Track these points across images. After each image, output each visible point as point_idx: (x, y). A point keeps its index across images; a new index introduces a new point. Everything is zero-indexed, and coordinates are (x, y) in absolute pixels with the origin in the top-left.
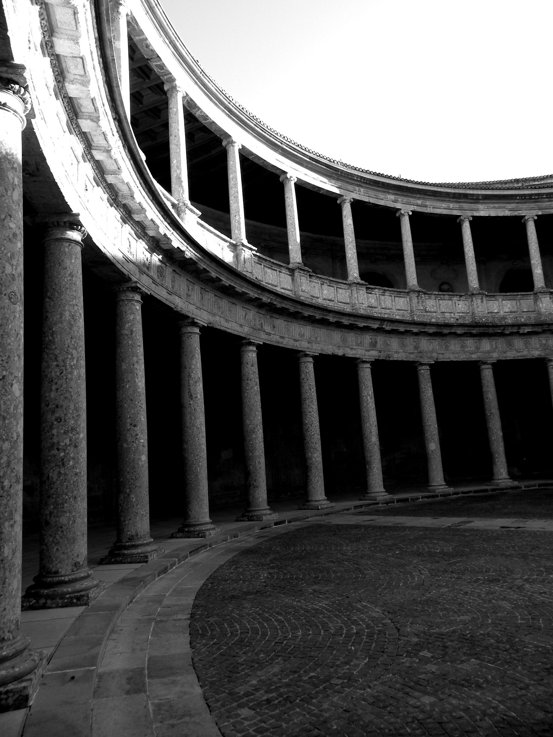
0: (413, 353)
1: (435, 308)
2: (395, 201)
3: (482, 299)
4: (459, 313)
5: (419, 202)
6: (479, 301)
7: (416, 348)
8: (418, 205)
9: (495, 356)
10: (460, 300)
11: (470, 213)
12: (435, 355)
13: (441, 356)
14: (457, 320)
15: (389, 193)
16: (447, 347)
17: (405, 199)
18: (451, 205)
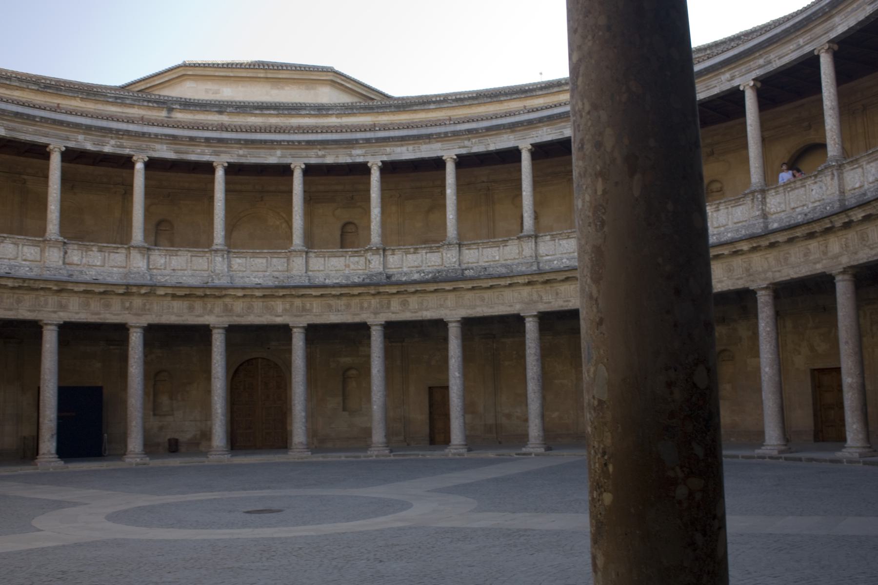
0: (741, 278)
1: (783, 206)
2: (732, 78)
3: (833, 174)
4: (813, 203)
5: (761, 61)
6: (829, 178)
7: (748, 270)
8: (760, 67)
9: (845, 261)
10: (816, 183)
11: (825, 39)
12: (770, 275)
13: (777, 275)
14: (806, 215)
15: (724, 73)
16: (786, 259)
17: (743, 68)
18: (801, 41)
